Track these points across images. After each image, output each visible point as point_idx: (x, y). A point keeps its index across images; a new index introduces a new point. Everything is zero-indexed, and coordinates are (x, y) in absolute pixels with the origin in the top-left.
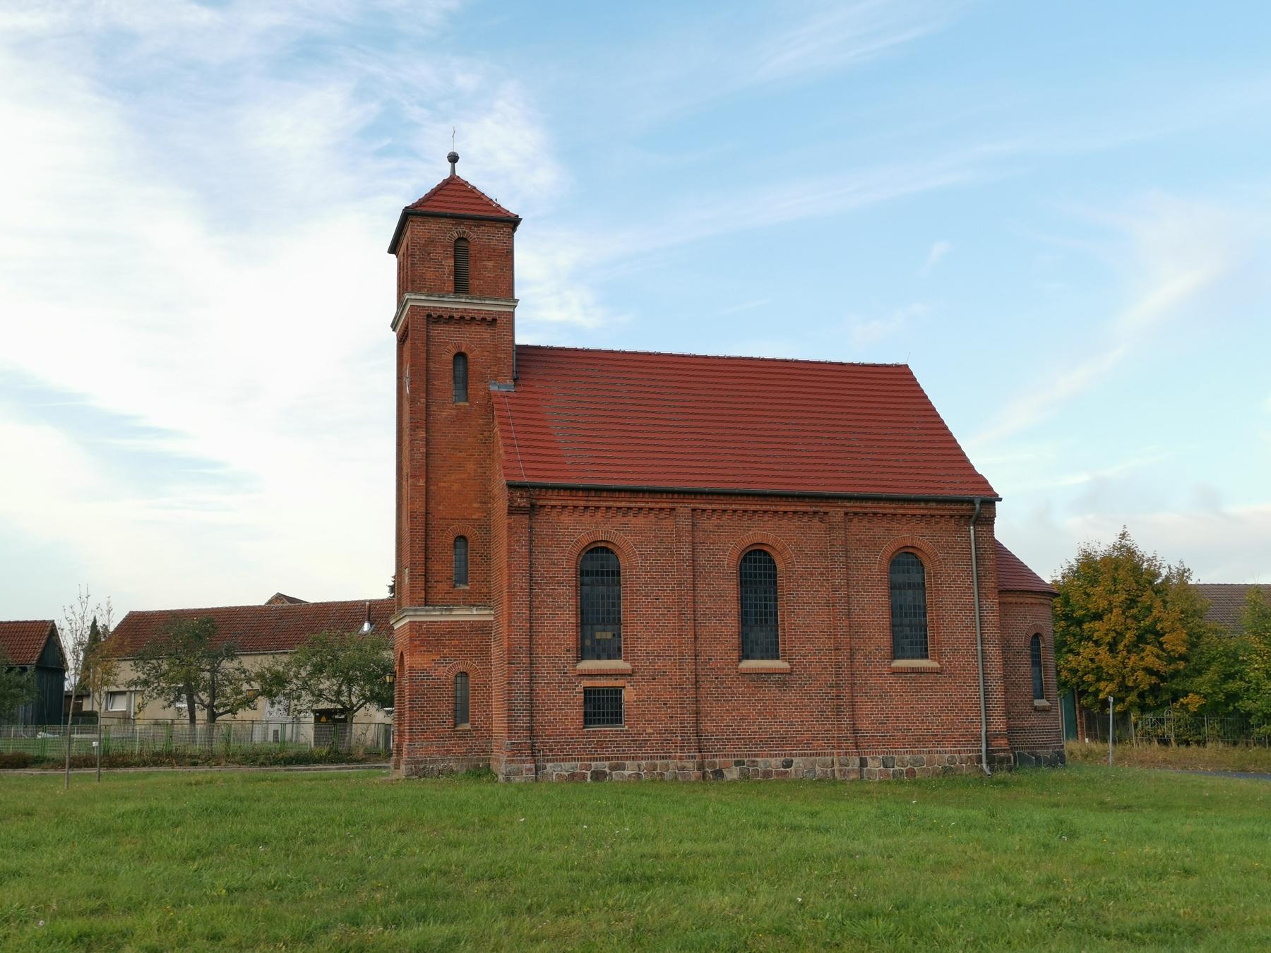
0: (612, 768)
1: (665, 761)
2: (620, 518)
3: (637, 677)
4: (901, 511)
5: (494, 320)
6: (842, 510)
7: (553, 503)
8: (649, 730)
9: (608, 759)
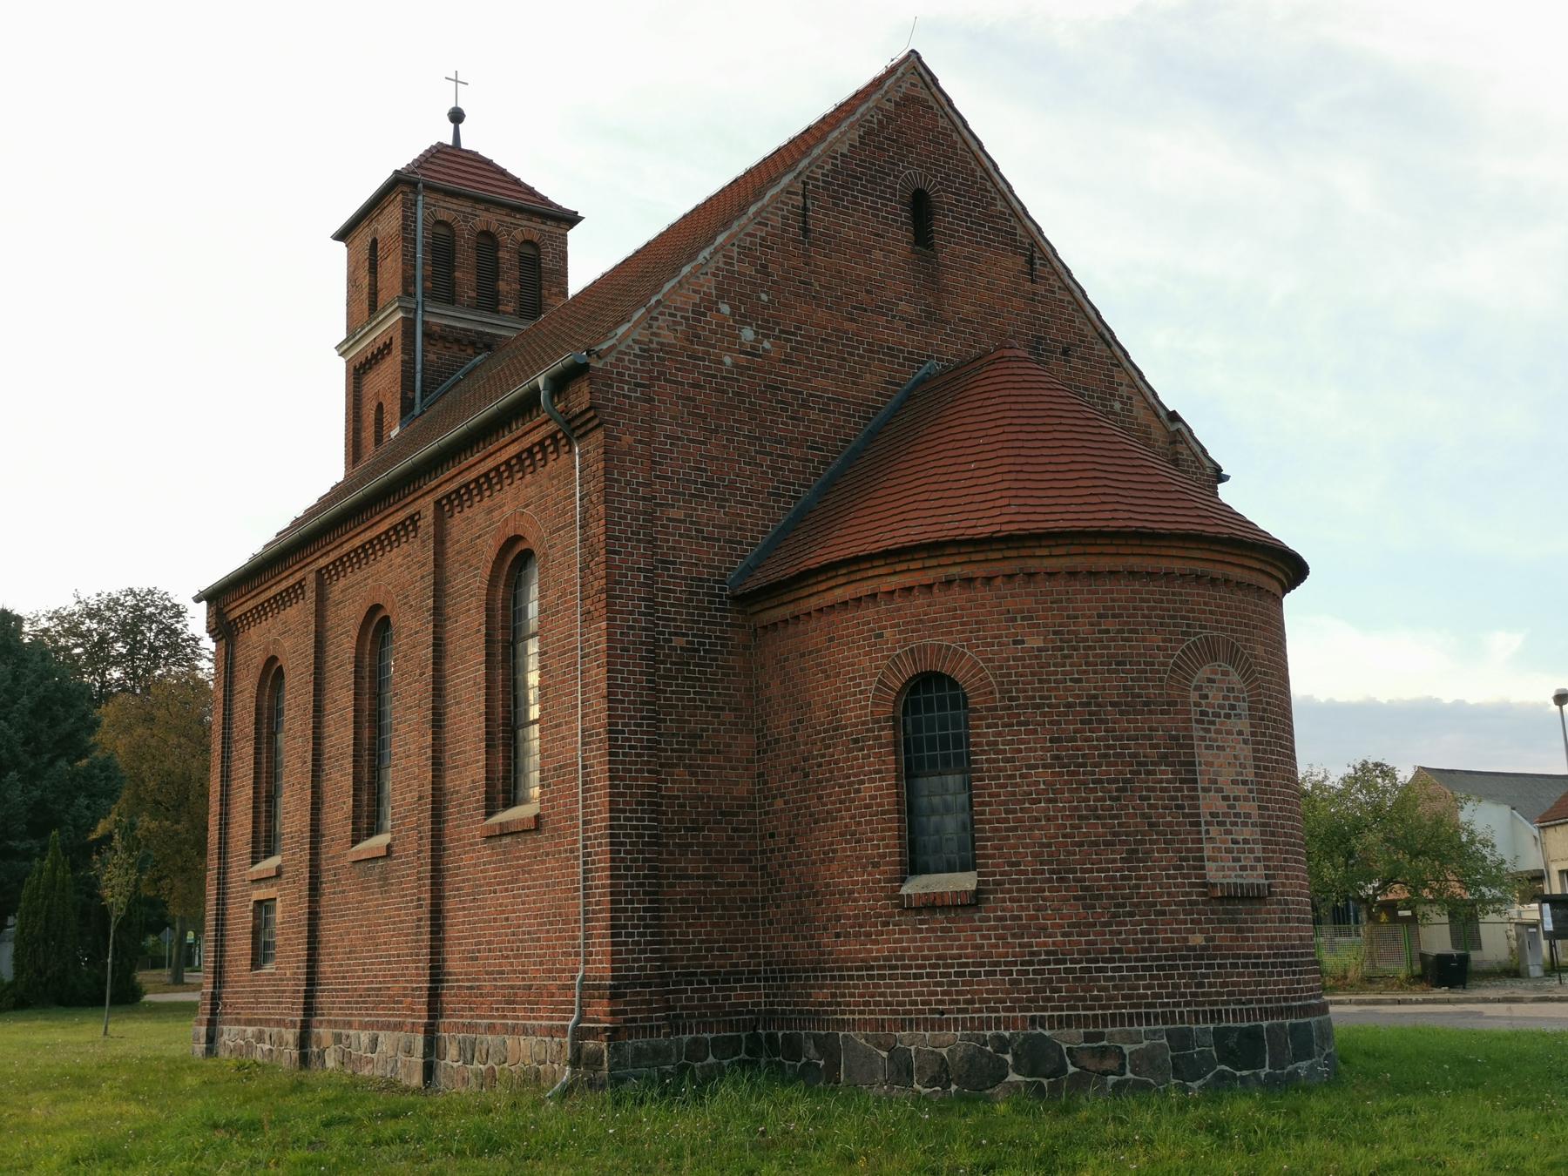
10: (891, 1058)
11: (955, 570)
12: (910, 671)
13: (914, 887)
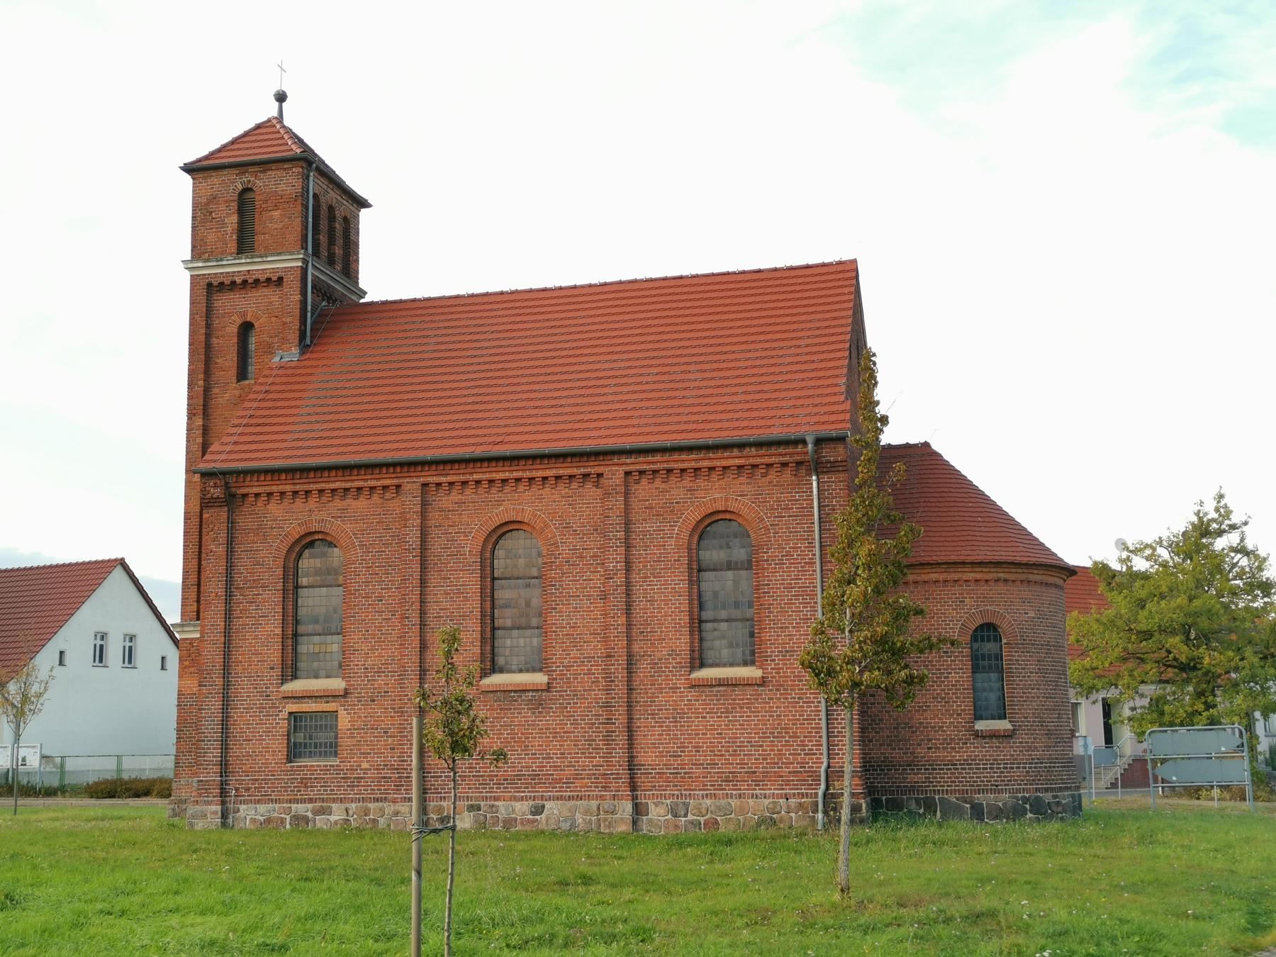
0: (317, 812)
1: (380, 804)
2: (338, 503)
3: (352, 699)
4: (706, 463)
5: (280, 279)
6: (622, 469)
7: (256, 490)
8: (365, 765)
9: (311, 801)
10: (972, 807)
11: (1002, 575)
12: (980, 622)
13: (981, 725)
